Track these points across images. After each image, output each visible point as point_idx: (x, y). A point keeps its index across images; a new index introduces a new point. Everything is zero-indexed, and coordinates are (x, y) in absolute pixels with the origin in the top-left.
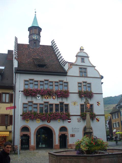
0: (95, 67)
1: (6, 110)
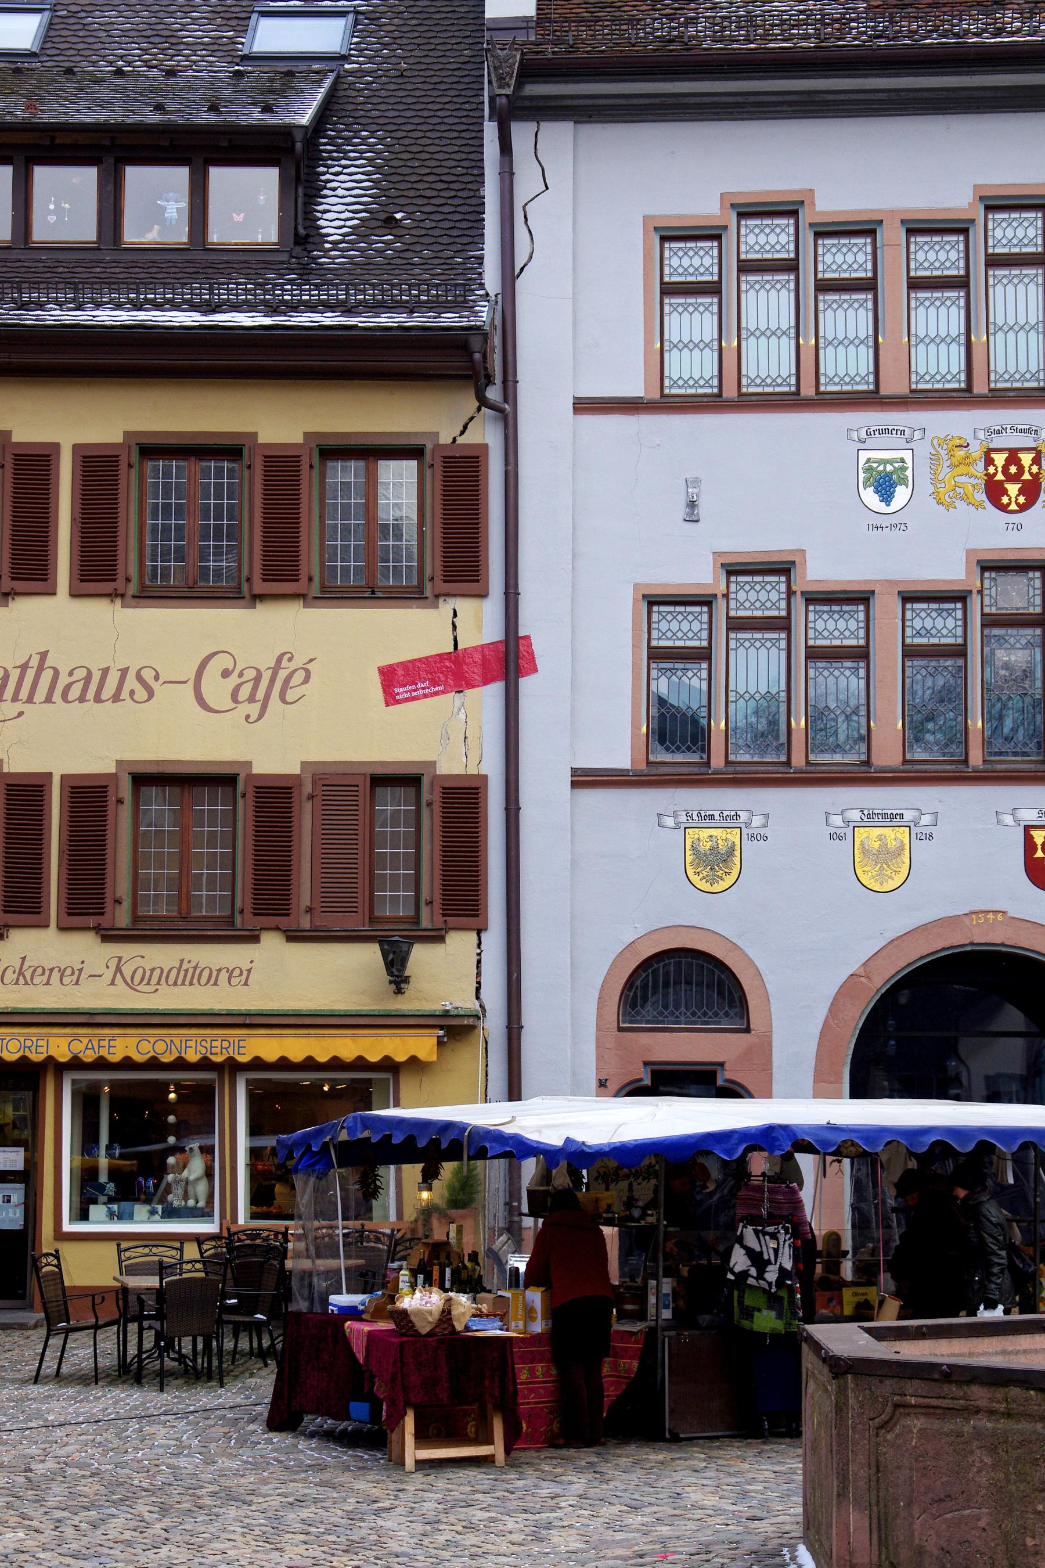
1: (391, 699)
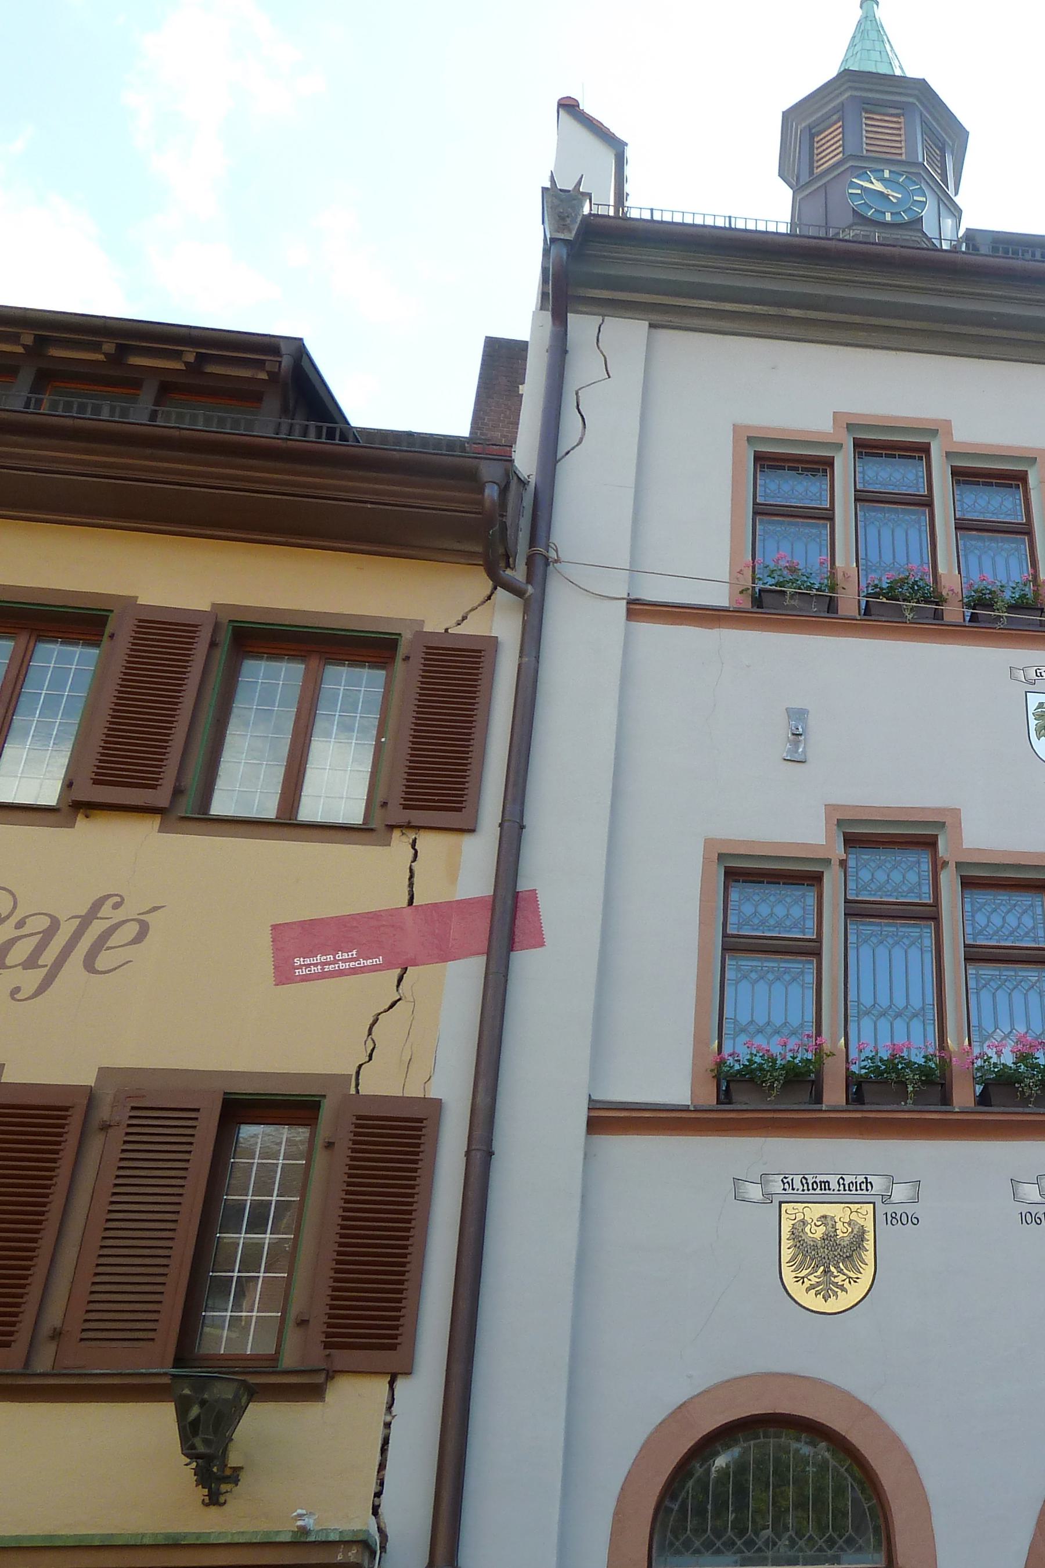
1: (284, 975)
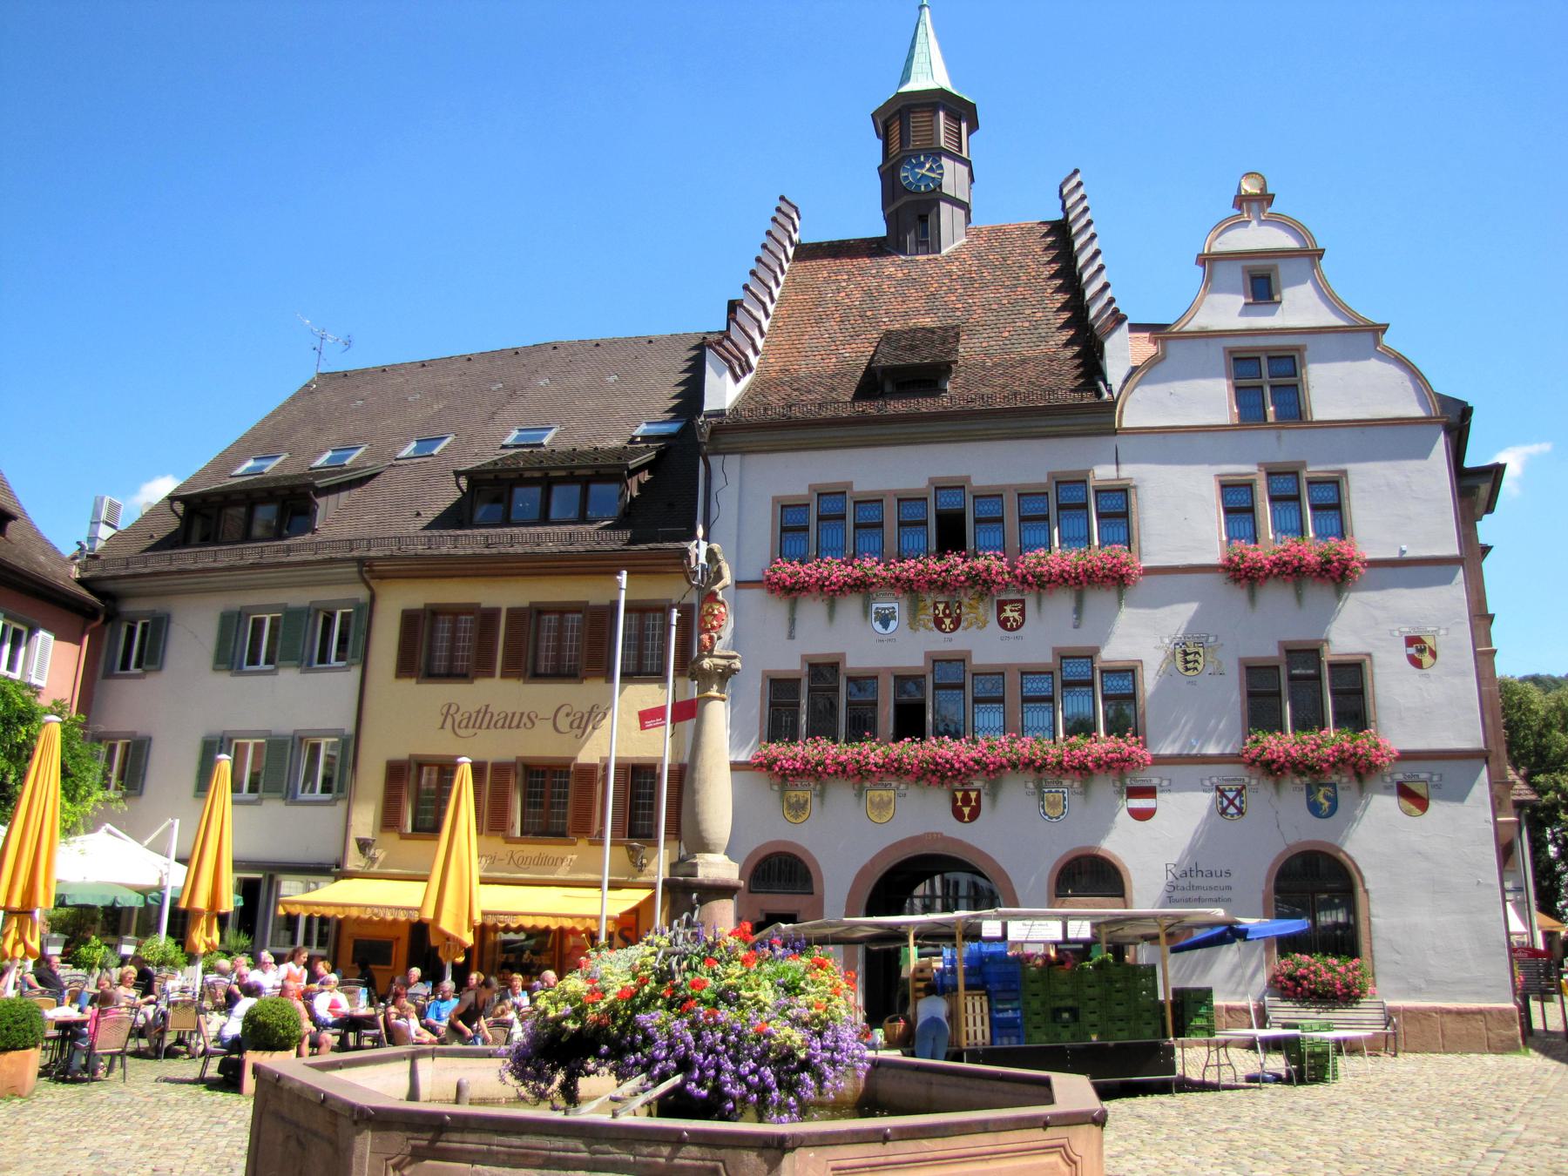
0: (1383, 328)
1: (643, 727)
